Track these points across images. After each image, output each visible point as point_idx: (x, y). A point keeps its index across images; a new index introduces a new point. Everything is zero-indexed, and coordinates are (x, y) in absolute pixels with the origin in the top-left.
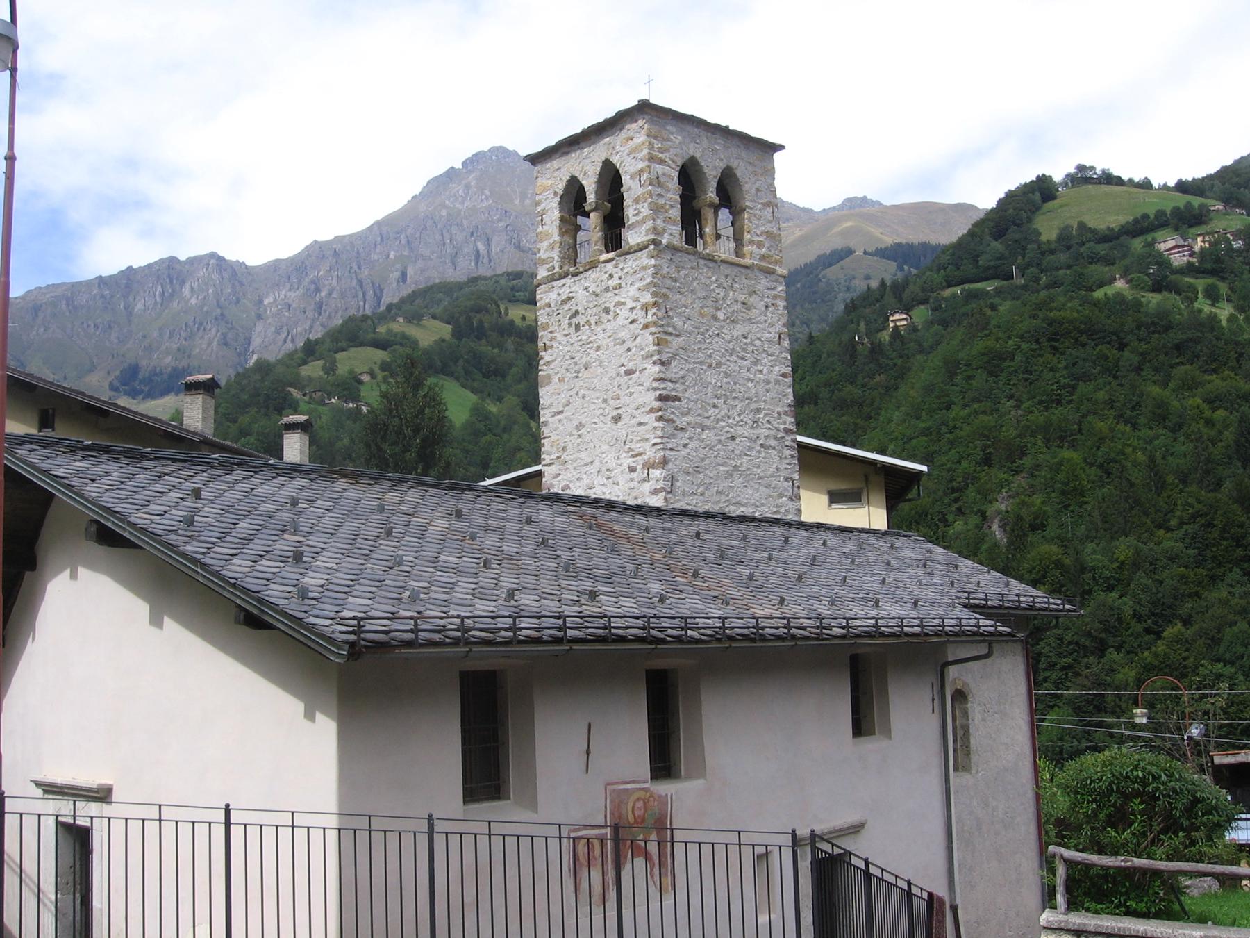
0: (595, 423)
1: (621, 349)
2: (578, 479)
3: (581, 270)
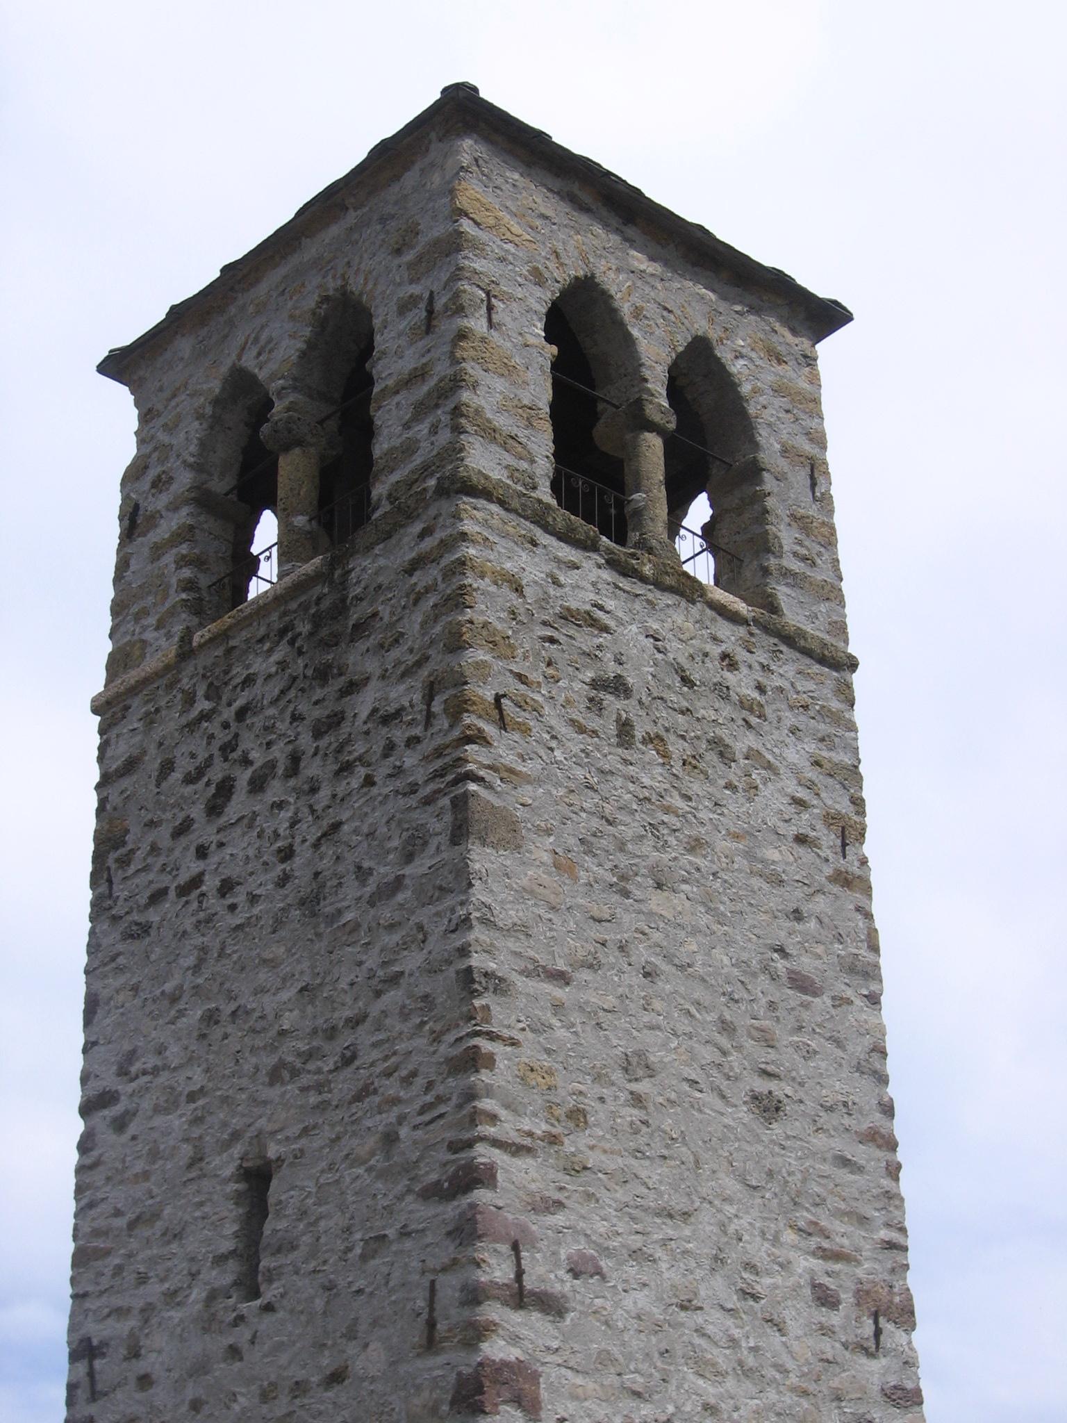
0: (693, 1083)
1: (775, 899)
2: (634, 1254)
3: (647, 570)
